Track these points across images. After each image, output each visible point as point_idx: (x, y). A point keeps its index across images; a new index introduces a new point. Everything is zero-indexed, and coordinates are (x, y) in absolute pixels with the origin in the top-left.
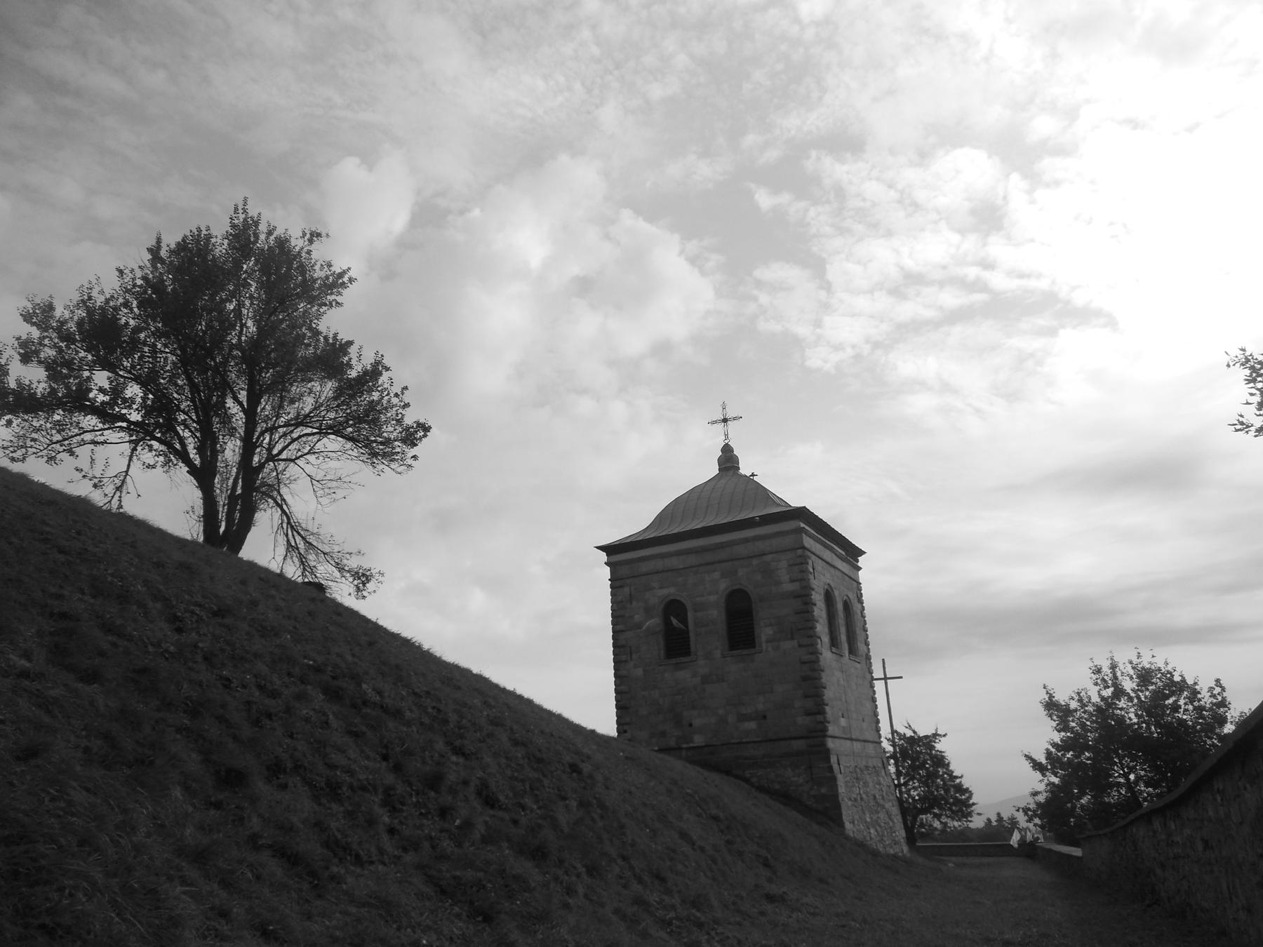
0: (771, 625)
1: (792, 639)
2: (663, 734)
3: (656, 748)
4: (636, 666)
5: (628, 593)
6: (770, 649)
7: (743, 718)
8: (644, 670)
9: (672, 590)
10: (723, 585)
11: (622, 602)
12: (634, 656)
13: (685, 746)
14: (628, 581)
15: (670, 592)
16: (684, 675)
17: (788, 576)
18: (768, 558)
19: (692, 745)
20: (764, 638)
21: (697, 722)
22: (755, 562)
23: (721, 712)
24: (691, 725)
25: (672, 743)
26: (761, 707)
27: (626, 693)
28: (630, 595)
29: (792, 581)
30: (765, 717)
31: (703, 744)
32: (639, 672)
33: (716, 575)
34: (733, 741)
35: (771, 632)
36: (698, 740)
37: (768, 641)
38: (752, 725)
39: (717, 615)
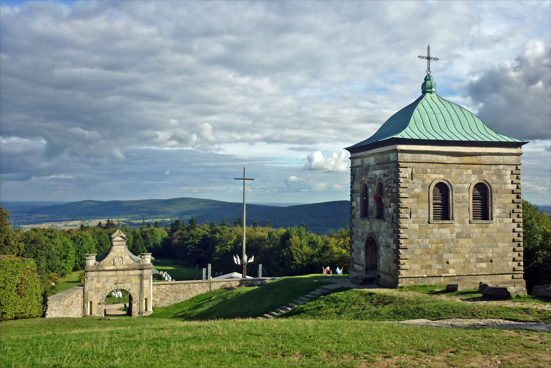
0: (500, 208)
1: (510, 217)
2: (430, 267)
3: (425, 276)
4: (413, 222)
5: (411, 173)
6: (498, 222)
7: (480, 260)
8: (419, 225)
9: (442, 176)
10: (475, 180)
11: (406, 178)
12: (413, 215)
13: (444, 275)
14: (411, 164)
15: (439, 177)
16: (445, 231)
17: (511, 180)
18: (501, 167)
19: (448, 275)
20: (494, 215)
21: (452, 261)
22: (493, 167)
23: (467, 256)
24: (448, 263)
25: (435, 273)
26: (490, 255)
27: (407, 239)
28: (412, 174)
29: (512, 183)
30: (491, 261)
31: (456, 275)
32: (416, 226)
33: (470, 171)
34: (473, 274)
35: (499, 212)
36: (452, 272)
37: (498, 217)
38: (484, 265)
39: (469, 196)
